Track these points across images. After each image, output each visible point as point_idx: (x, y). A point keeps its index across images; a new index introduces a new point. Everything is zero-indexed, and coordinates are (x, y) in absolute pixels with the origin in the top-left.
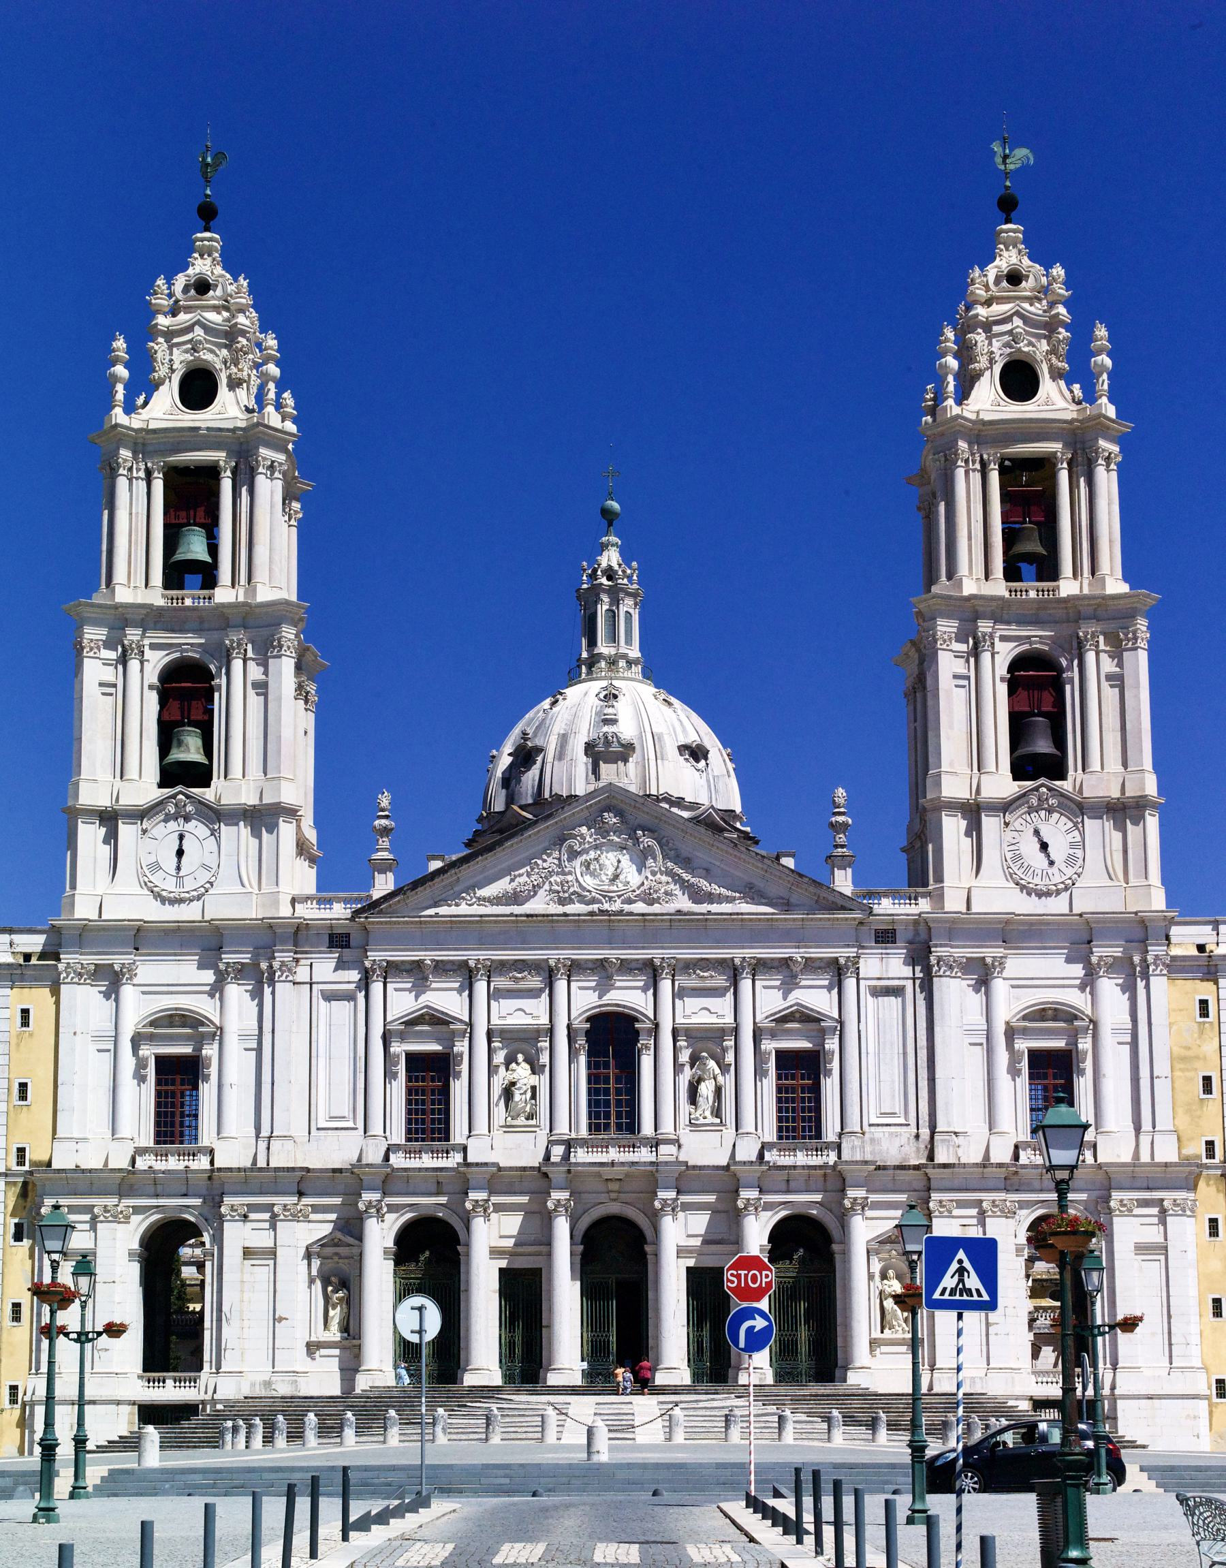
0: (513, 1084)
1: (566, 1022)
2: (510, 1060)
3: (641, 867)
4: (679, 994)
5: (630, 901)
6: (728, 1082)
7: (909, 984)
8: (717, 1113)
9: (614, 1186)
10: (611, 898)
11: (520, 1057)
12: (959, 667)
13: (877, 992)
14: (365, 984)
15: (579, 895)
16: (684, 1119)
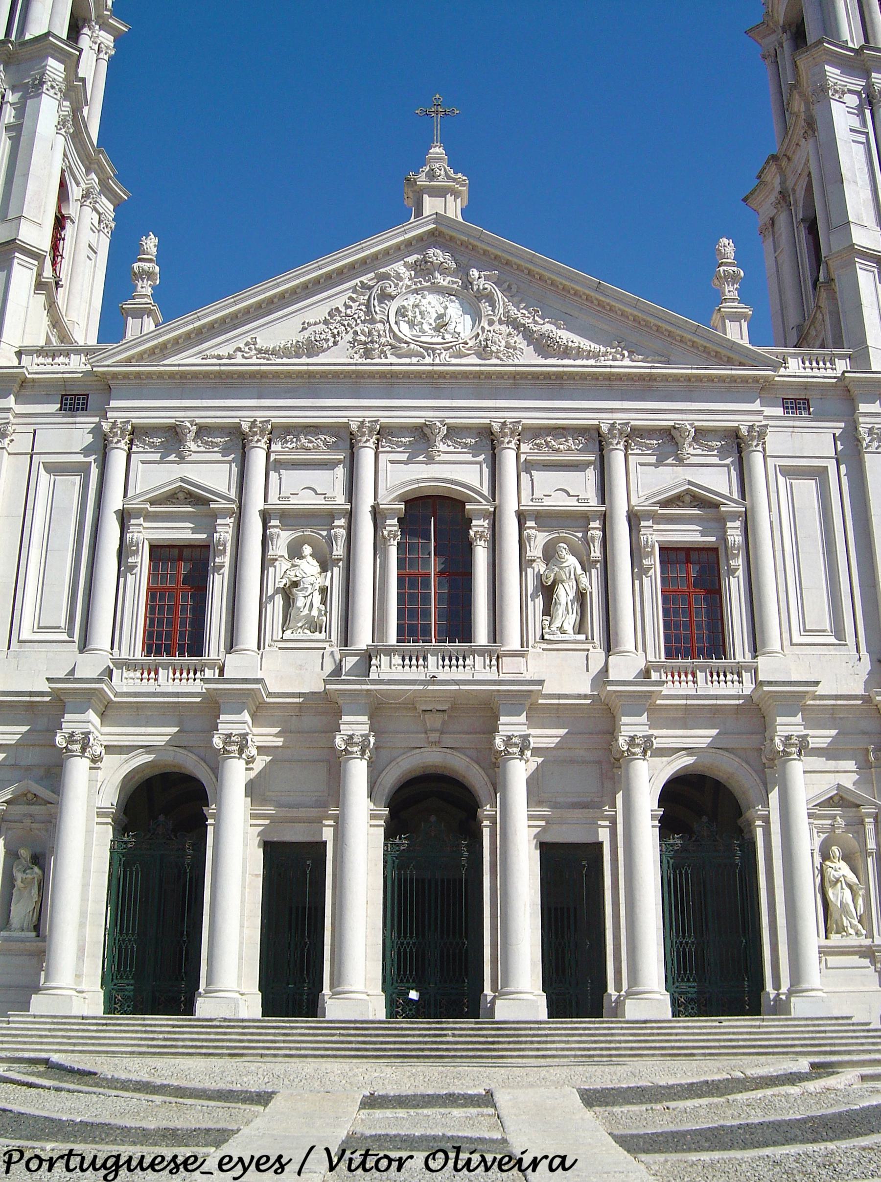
0: (295, 584)
1: (371, 502)
2: (295, 552)
3: (476, 316)
4: (526, 467)
5: (460, 355)
6: (592, 583)
7: (832, 465)
8: (580, 628)
9: (436, 721)
10: (434, 350)
11: (307, 550)
12: (855, 122)
13: (790, 472)
14: (102, 447)
15: (393, 347)
16: (533, 635)
